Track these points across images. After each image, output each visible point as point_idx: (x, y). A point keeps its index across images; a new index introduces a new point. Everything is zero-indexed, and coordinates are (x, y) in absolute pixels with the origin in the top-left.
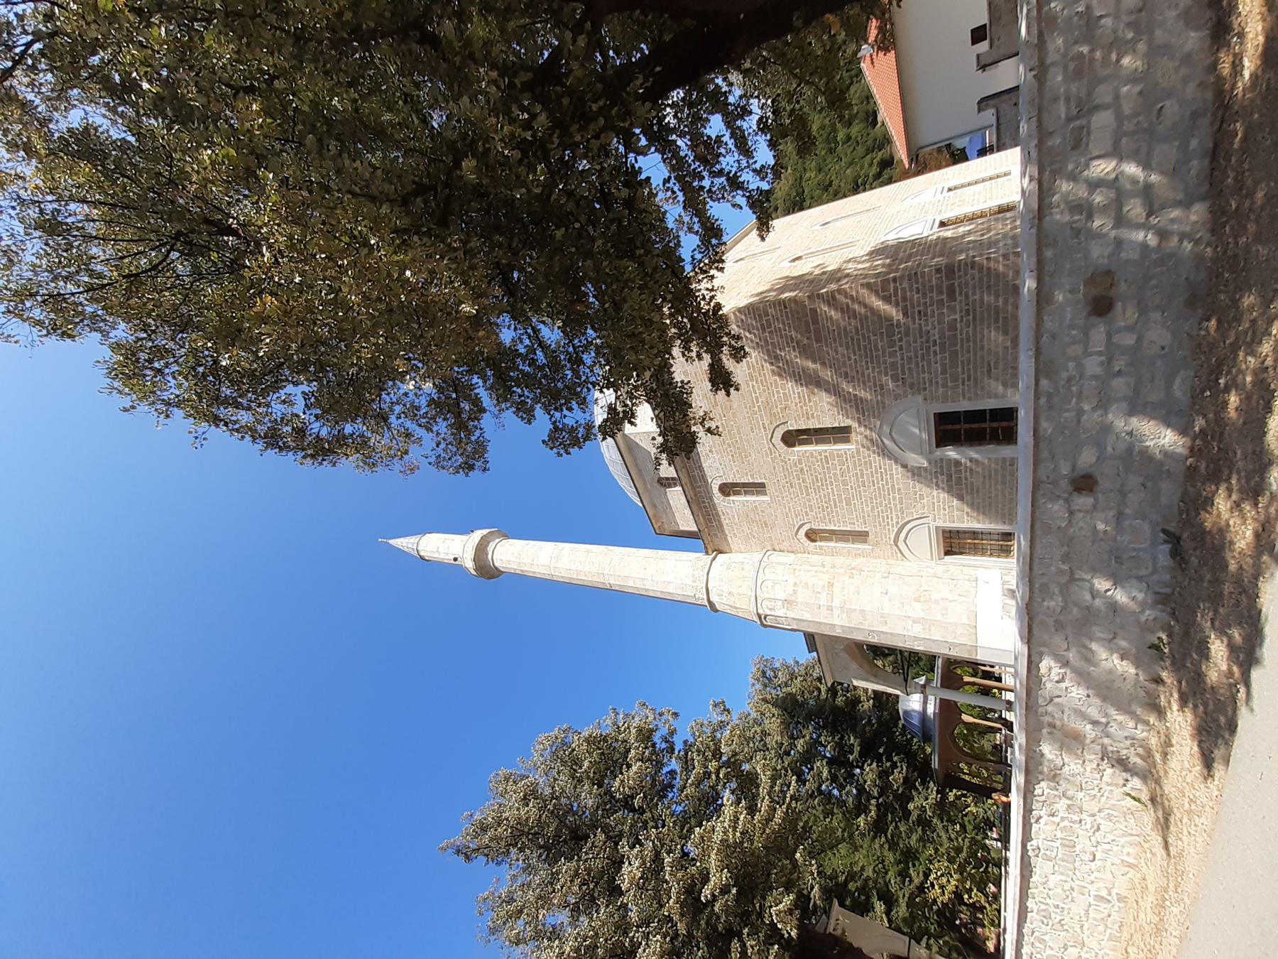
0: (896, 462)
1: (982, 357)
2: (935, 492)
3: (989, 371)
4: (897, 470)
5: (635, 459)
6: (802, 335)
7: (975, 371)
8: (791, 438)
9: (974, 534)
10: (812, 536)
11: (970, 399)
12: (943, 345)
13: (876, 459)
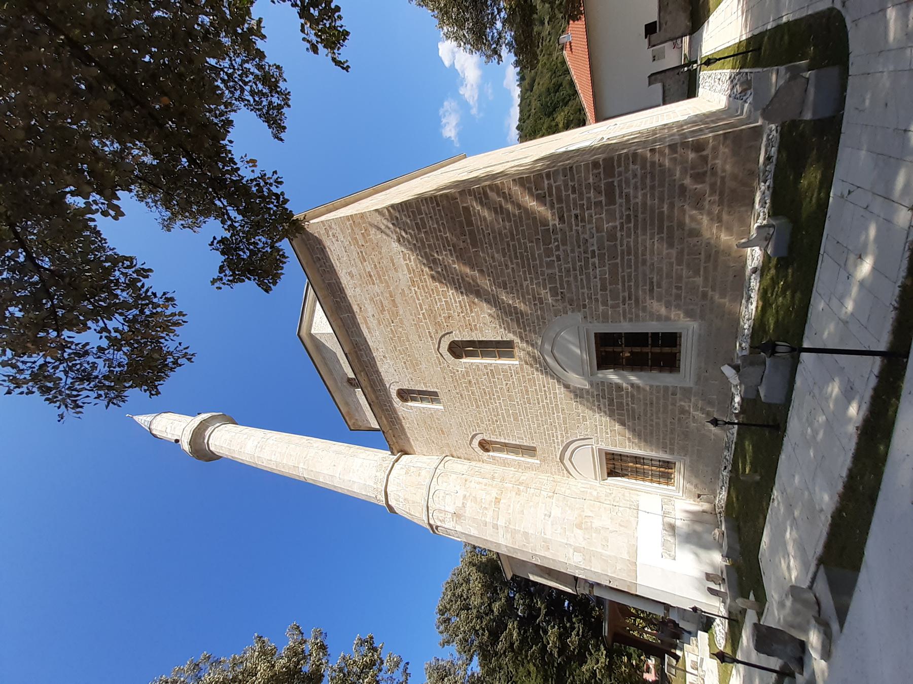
0: (559, 381)
1: (645, 275)
2: (597, 416)
3: (651, 290)
4: (560, 390)
6: (458, 239)
7: (637, 287)
8: (458, 349)
9: (636, 459)
10: (485, 446)
11: (631, 320)
12: (601, 257)
13: (540, 377)
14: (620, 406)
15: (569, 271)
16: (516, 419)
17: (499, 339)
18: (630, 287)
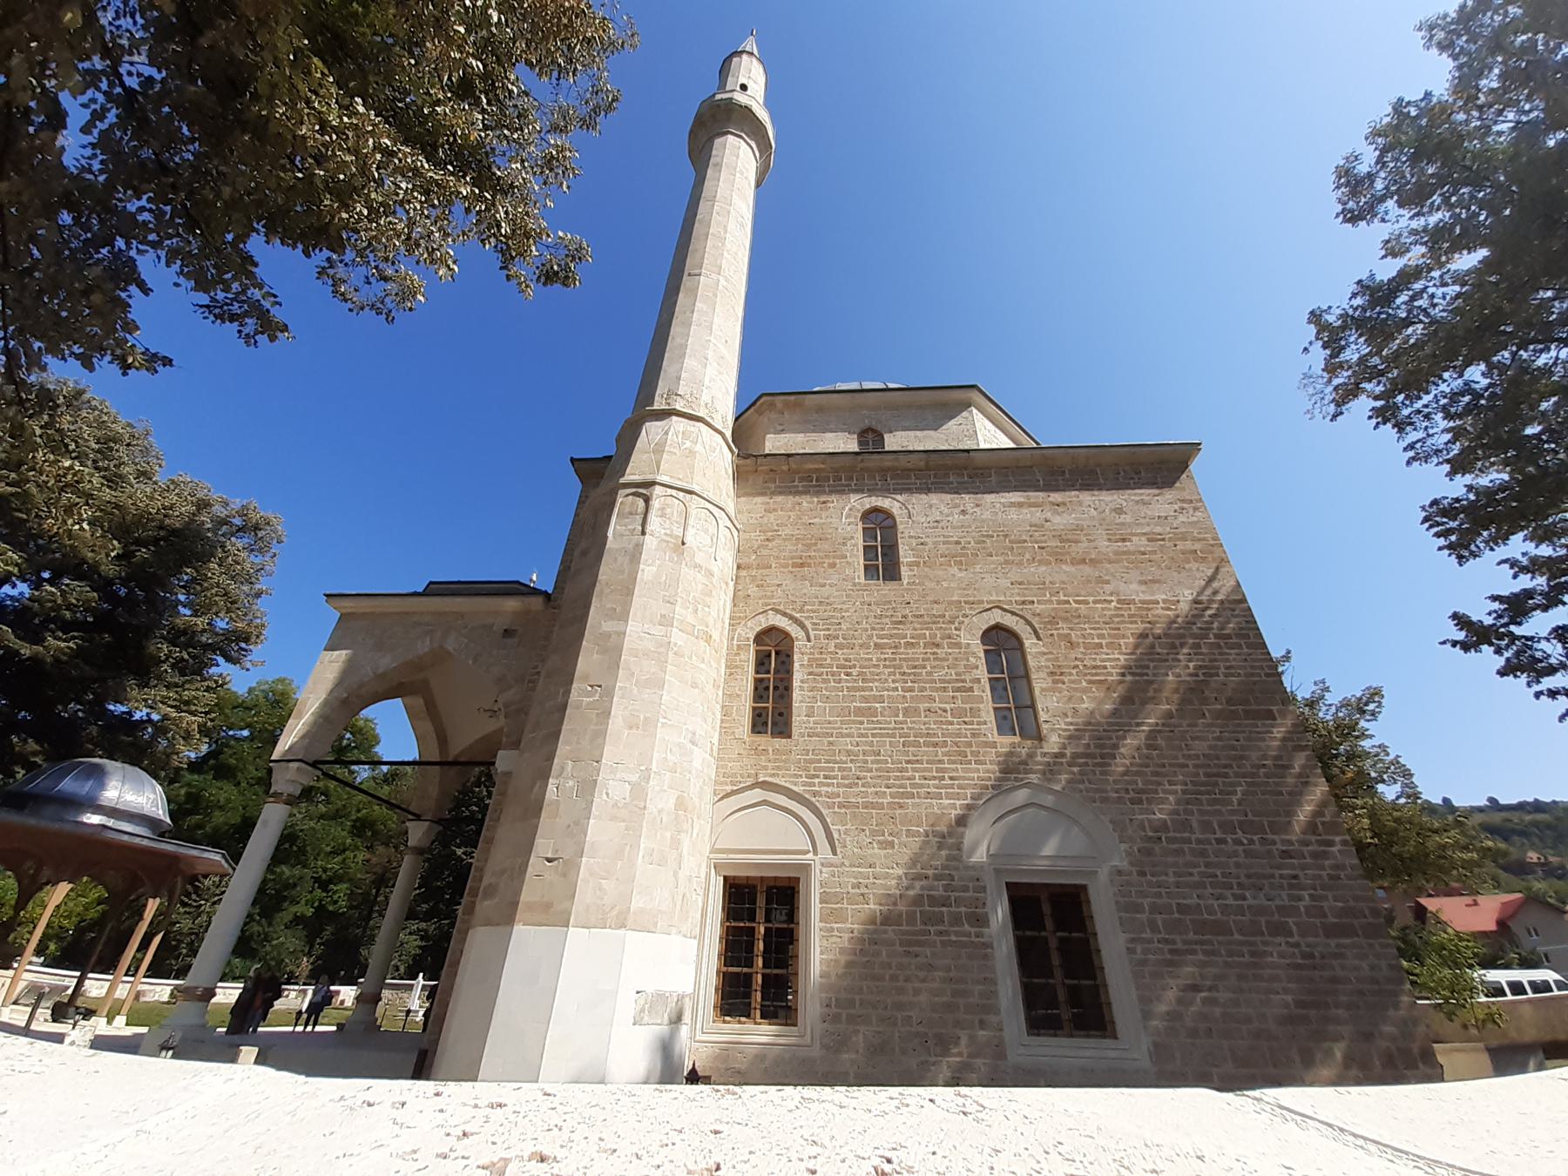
0: (969, 807)
4: (952, 807)
5: (921, 407)
11: (1131, 951)
14: (928, 919)
15: (1203, 853)
16: (859, 712)
17: (1043, 716)
18: (1194, 952)
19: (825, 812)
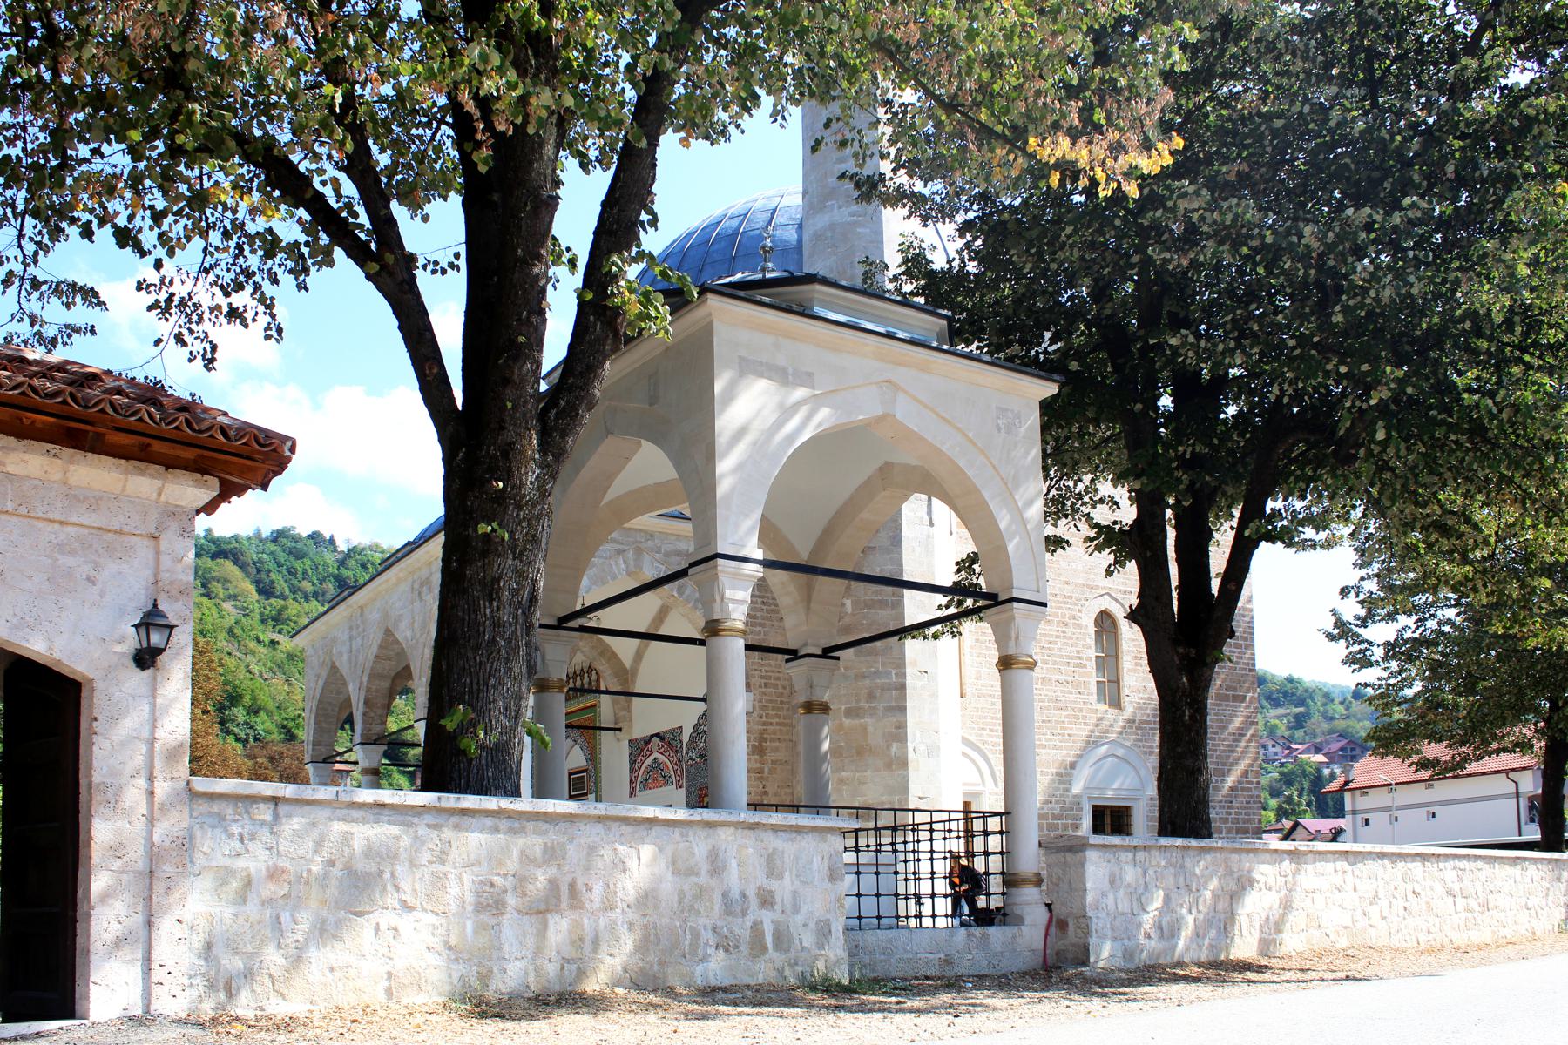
6: (1224, 680)
13: (1081, 732)
19: (991, 757)
